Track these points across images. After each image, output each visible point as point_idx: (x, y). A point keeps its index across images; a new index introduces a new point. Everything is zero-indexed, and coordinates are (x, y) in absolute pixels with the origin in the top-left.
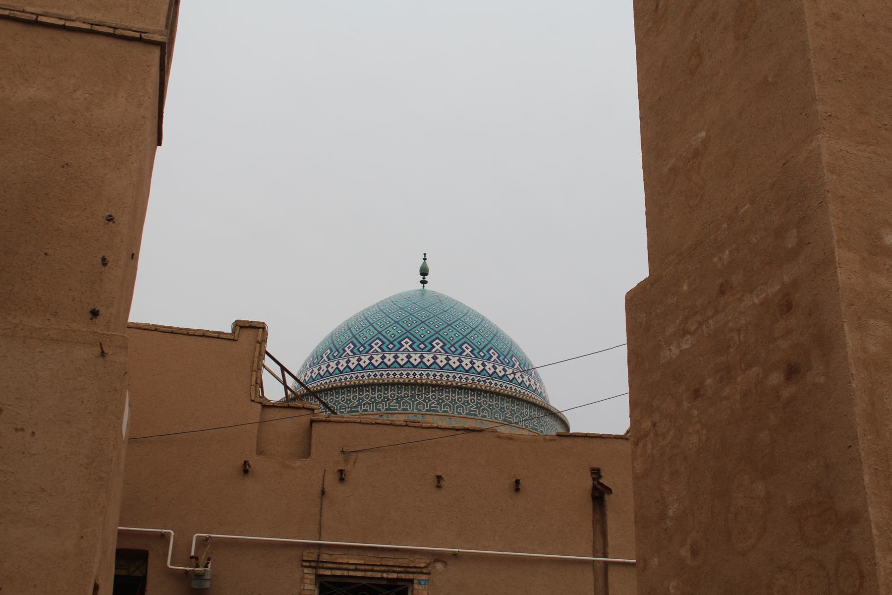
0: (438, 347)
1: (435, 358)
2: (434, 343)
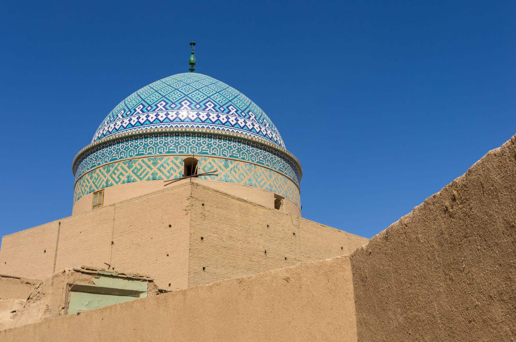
0: (210, 107)
2: (207, 105)
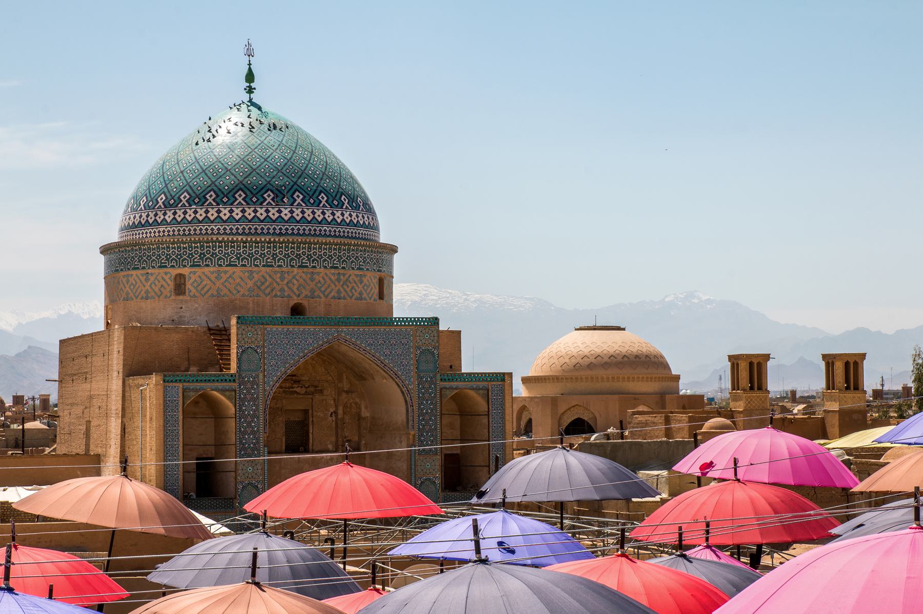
1: (267, 211)
